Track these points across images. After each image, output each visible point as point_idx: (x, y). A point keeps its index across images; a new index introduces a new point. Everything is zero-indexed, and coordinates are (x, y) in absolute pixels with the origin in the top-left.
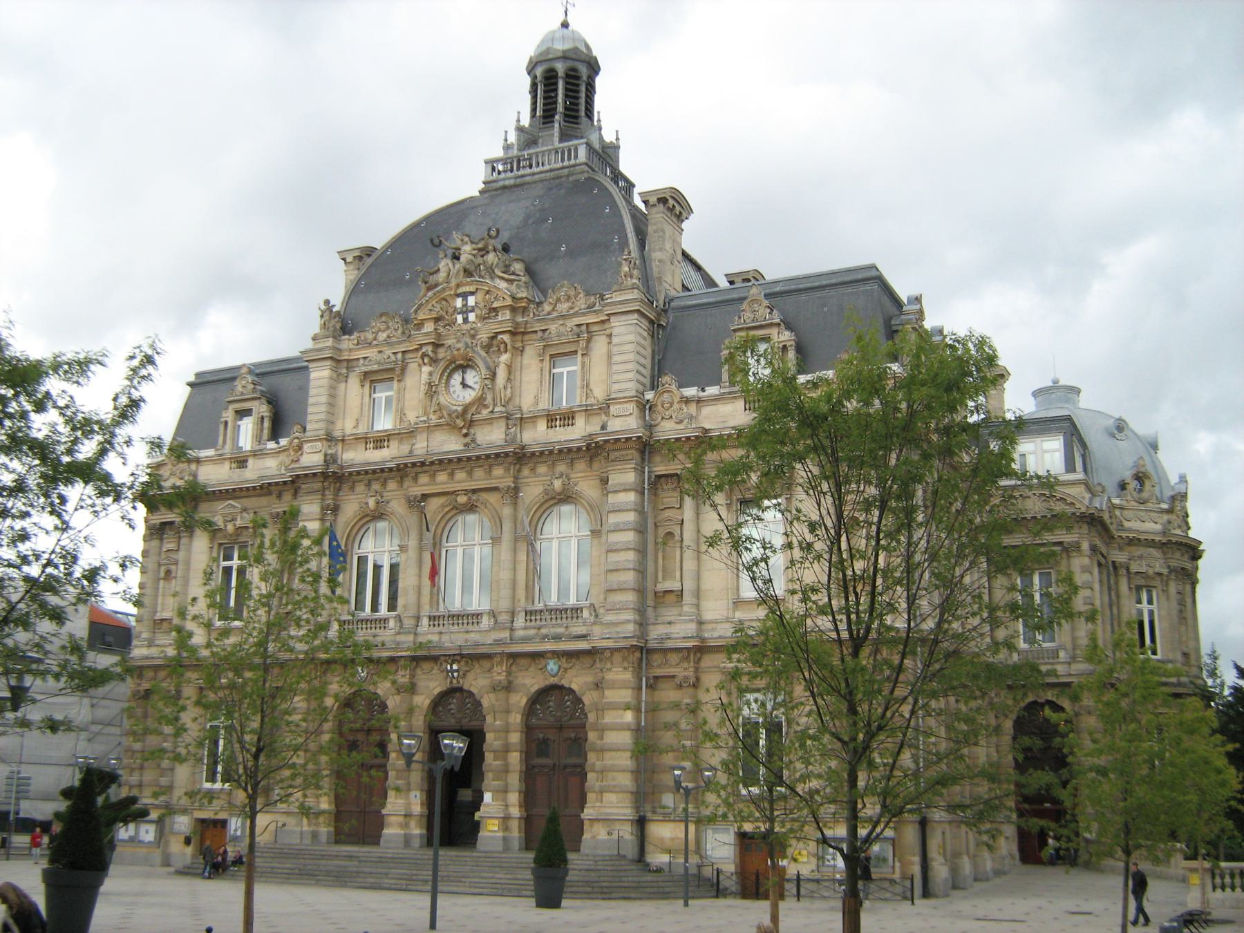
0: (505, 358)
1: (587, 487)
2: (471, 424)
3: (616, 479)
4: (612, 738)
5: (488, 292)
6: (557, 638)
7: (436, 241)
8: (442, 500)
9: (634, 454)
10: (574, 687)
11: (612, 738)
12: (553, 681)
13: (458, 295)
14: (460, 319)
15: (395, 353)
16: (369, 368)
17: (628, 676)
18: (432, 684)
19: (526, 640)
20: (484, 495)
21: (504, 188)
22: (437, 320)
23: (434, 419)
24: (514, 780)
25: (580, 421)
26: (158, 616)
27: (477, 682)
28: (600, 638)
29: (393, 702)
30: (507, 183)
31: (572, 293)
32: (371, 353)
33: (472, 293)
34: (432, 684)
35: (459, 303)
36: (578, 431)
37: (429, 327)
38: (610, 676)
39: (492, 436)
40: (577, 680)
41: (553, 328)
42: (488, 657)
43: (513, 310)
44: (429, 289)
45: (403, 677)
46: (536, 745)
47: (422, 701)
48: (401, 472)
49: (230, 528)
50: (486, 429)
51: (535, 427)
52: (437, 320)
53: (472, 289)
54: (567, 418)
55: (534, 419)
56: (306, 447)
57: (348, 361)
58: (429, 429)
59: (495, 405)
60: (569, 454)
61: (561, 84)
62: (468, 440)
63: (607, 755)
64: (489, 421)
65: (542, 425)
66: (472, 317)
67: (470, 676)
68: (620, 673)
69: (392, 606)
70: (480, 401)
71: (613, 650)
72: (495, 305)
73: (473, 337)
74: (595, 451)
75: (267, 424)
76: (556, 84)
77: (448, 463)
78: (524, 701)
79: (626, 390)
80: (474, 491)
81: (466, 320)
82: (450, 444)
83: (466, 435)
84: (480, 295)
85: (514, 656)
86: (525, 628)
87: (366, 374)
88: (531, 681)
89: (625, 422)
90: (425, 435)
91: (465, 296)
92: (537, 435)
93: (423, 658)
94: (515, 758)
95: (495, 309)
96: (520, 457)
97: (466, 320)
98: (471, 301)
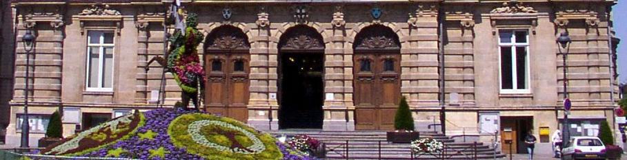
17: (434, 21)
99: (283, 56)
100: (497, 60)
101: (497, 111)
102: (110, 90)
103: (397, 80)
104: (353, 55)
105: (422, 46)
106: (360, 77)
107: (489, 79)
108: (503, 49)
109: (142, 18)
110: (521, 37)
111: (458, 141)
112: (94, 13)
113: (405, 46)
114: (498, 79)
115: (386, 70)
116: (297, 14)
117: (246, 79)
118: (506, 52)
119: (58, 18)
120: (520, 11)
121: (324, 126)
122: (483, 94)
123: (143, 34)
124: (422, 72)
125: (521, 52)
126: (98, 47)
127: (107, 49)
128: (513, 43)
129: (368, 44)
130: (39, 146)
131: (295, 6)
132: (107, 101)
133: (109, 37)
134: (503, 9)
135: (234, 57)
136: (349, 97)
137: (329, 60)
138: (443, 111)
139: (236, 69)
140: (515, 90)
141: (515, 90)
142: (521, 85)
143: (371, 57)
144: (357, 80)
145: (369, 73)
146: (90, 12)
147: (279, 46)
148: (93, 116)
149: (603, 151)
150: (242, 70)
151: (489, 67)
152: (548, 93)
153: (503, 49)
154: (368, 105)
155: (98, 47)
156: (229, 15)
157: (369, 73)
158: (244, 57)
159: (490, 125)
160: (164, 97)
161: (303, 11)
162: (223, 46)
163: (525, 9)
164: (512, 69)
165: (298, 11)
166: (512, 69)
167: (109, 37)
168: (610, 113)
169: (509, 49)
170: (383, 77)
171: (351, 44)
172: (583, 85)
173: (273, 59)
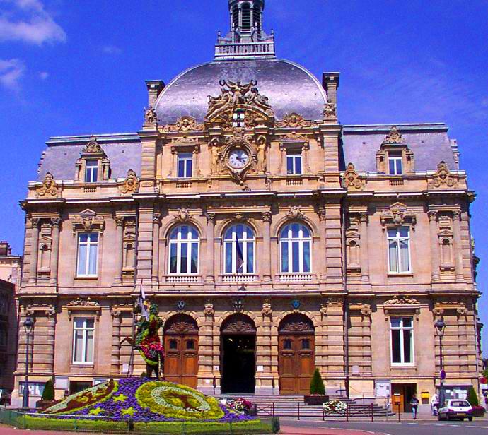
0: (262, 147)
3: (329, 213)
13: (234, 112)
14: (235, 124)
15: (194, 139)
17: (341, 310)
21: (228, 60)
23: (223, 176)
26: (39, 270)
35: (235, 116)
36: (306, 188)
39: (258, 187)
44: (217, 107)
48: (202, 203)
49: (88, 223)
52: (221, 124)
54: (299, 180)
61: (240, 14)
62: (243, 187)
65: (284, 182)
66: (242, 124)
69: (194, 270)
70: (249, 168)
72: (256, 120)
75: (107, 169)
76: (249, 11)
79: (332, 170)
81: (239, 126)
82: (232, 189)
83: (242, 185)
87: (177, 148)
89: (333, 186)
92: (282, 188)
96: (275, 201)
97: (239, 126)
98: (242, 116)
99: (224, 337)
100: (389, 340)
101: (388, 380)
102: (91, 363)
103: (312, 355)
104: (278, 336)
105: (331, 329)
106: (301, 353)
107: (382, 355)
108: (393, 331)
109: (116, 308)
110: (407, 322)
111: (359, 402)
112: (79, 304)
113: (317, 330)
114: (390, 355)
115: (303, 348)
116: (235, 305)
117: (196, 355)
118: (396, 334)
119: (51, 308)
120: (407, 302)
121: (256, 391)
122: (378, 366)
123: (116, 320)
124: (331, 350)
125: (407, 335)
126: (82, 330)
127: (89, 332)
128: (401, 327)
129: (290, 328)
130: (37, 407)
131: (234, 298)
132: (89, 372)
133: (90, 323)
134: (393, 301)
135: (186, 338)
136: (275, 369)
137: (259, 340)
138: (347, 380)
139: (188, 348)
140: (403, 364)
141: (403, 364)
142: (407, 359)
143: (291, 338)
144: (281, 355)
145: (290, 351)
146: (75, 303)
147: (221, 330)
148: (78, 384)
149: (470, 410)
150: (193, 348)
151: (383, 345)
152: (428, 366)
153: (393, 331)
154: (290, 375)
155: (82, 330)
156: (183, 306)
157: (290, 351)
158: (194, 338)
159: (383, 390)
160: (133, 369)
161: (240, 303)
162: (178, 330)
163: (410, 301)
164: (400, 348)
165: (236, 303)
166: (400, 348)
167: (90, 323)
168: (475, 381)
169: (399, 331)
170: (301, 353)
171: (277, 328)
172: (455, 360)
173: (217, 339)
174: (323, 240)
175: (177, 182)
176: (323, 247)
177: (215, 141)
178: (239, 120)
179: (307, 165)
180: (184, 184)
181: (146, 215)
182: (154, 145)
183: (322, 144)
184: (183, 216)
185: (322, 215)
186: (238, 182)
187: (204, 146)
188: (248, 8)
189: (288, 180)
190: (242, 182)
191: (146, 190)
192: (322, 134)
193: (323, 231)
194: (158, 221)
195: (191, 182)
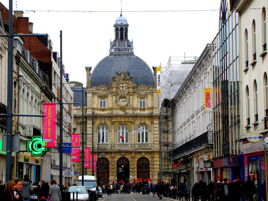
0: (131, 97)
1: (148, 122)
2: (125, 109)
4: (155, 166)
5: (127, 84)
6: (144, 149)
7: (117, 73)
8: (118, 123)
9: (158, 118)
10: (147, 157)
11: (155, 166)
12: (143, 156)
13: (121, 84)
14: (121, 88)
16: (101, 95)
17: (158, 156)
18: (118, 157)
19: (137, 149)
20: (127, 123)
22: (116, 88)
23: (117, 107)
24: (136, 173)
25: (146, 110)
27: (128, 156)
28: (153, 149)
29: (110, 160)
30: (116, 54)
31: (144, 86)
32: (101, 92)
33: (124, 84)
34: (118, 156)
36: (147, 112)
37: (114, 89)
38: (155, 156)
39: (130, 112)
40: (147, 156)
41: (141, 92)
42: (131, 152)
43: (133, 88)
45: (113, 155)
46: (139, 167)
47: (116, 159)
48: (110, 117)
50: (128, 110)
51: (137, 111)
53: (124, 83)
54: (144, 110)
55: (137, 109)
56: (88, 110)
57: (95, 93)
58: (116, 109)
59: (130, 106)
60: (144, 117)
62: (125, 112)
63: (155, 169)
64: (129, 109)
65: (139, 110)
66: (124, 88)
67: (126, 155)
68: (157, 156)
70: (127, 105)
71: (156, 152)
72: (129, 87)
73: (124, 92)
74: (151, 117)
76: (123, 31)
77: (121, 116)
78: (137, 160)
80: (125, 122)
81: (123, 89)
82: (121, 113)
83: (124, 111)
84: (126, 84)
85: (135, 152)
86: (138, 147)
87: (99, 96)
88: (139, 156)
90: (115, 110)
91: (123, 84)
92: (138, 112)
93: (119, 152)
94: (136, 170)
95: (129, 88)
96: (136, 117)
97: (123, 89)
105: (155, 163)
113: (150, 163)
174: (152, 132)
175: (100, 109)
176: (152, 134)
177: (114, 94)
178: (123, 87)
179: (147, 104)
180: (103, 110)
181: (89, 122)
182: (91, 95)
183: (152, 96)
184: (103, 122)
185: (152, 123)
186: (123, 110)
187: (110, 96)
188: (123, 29)
189: (140, 109)
190: (124, 110)
191: (89, 112)
192: (153, 92)
193: (152, 129)
194: (93, 123)
195: (105, 109)
